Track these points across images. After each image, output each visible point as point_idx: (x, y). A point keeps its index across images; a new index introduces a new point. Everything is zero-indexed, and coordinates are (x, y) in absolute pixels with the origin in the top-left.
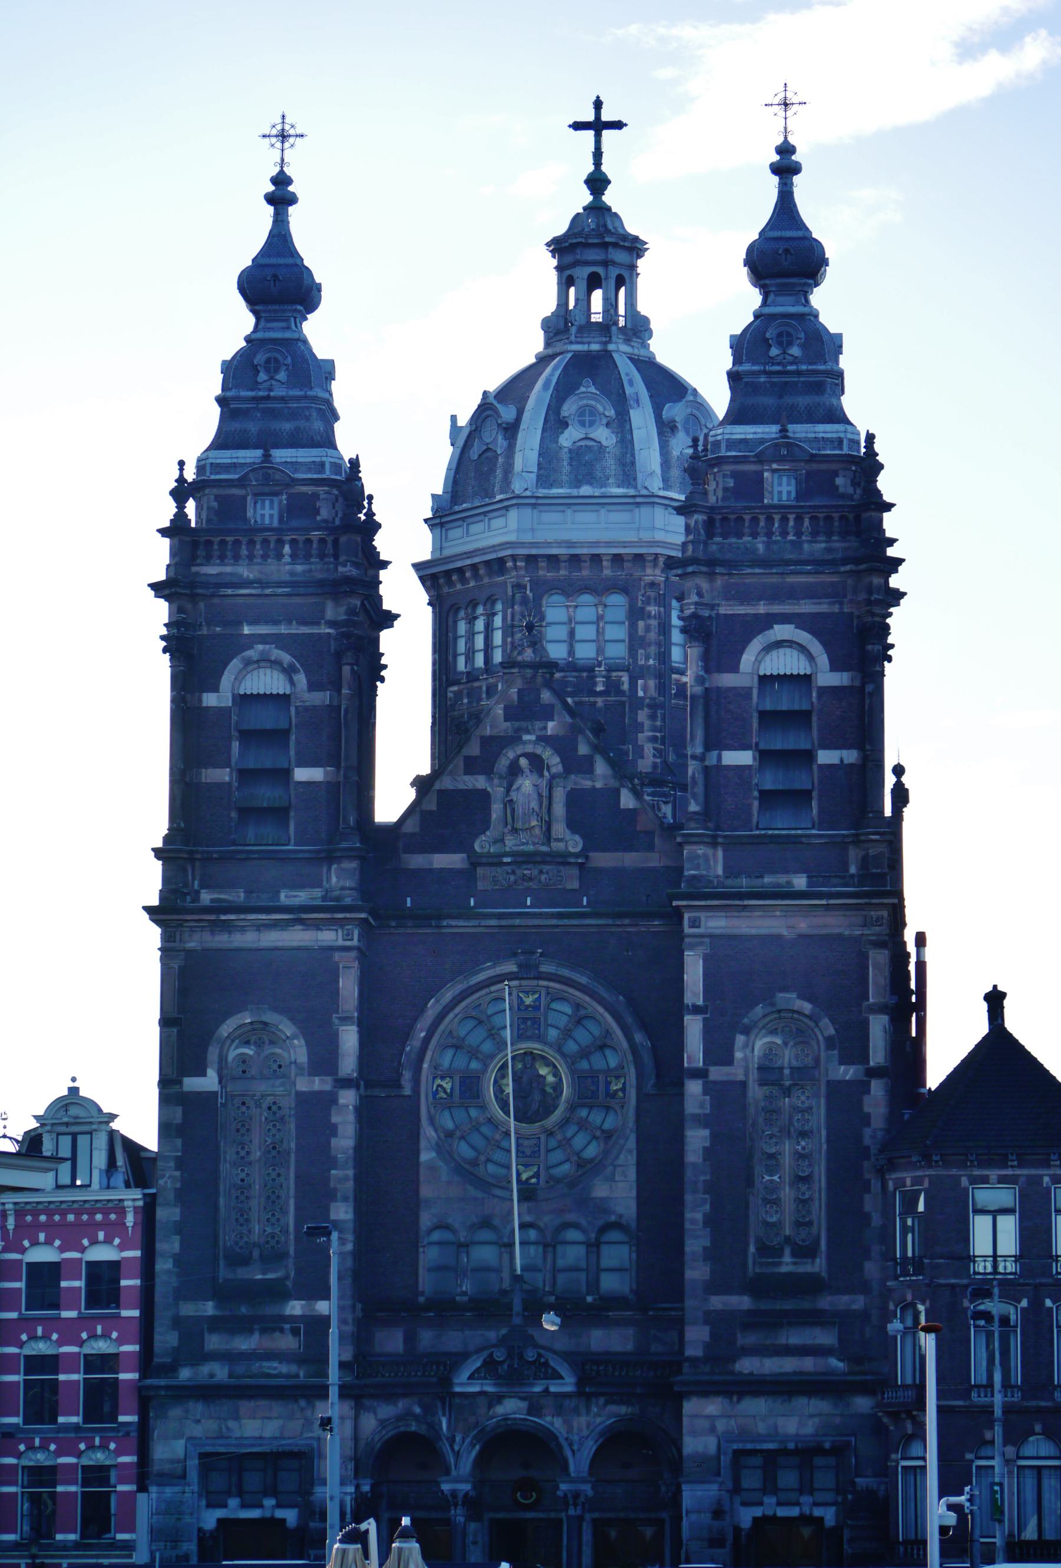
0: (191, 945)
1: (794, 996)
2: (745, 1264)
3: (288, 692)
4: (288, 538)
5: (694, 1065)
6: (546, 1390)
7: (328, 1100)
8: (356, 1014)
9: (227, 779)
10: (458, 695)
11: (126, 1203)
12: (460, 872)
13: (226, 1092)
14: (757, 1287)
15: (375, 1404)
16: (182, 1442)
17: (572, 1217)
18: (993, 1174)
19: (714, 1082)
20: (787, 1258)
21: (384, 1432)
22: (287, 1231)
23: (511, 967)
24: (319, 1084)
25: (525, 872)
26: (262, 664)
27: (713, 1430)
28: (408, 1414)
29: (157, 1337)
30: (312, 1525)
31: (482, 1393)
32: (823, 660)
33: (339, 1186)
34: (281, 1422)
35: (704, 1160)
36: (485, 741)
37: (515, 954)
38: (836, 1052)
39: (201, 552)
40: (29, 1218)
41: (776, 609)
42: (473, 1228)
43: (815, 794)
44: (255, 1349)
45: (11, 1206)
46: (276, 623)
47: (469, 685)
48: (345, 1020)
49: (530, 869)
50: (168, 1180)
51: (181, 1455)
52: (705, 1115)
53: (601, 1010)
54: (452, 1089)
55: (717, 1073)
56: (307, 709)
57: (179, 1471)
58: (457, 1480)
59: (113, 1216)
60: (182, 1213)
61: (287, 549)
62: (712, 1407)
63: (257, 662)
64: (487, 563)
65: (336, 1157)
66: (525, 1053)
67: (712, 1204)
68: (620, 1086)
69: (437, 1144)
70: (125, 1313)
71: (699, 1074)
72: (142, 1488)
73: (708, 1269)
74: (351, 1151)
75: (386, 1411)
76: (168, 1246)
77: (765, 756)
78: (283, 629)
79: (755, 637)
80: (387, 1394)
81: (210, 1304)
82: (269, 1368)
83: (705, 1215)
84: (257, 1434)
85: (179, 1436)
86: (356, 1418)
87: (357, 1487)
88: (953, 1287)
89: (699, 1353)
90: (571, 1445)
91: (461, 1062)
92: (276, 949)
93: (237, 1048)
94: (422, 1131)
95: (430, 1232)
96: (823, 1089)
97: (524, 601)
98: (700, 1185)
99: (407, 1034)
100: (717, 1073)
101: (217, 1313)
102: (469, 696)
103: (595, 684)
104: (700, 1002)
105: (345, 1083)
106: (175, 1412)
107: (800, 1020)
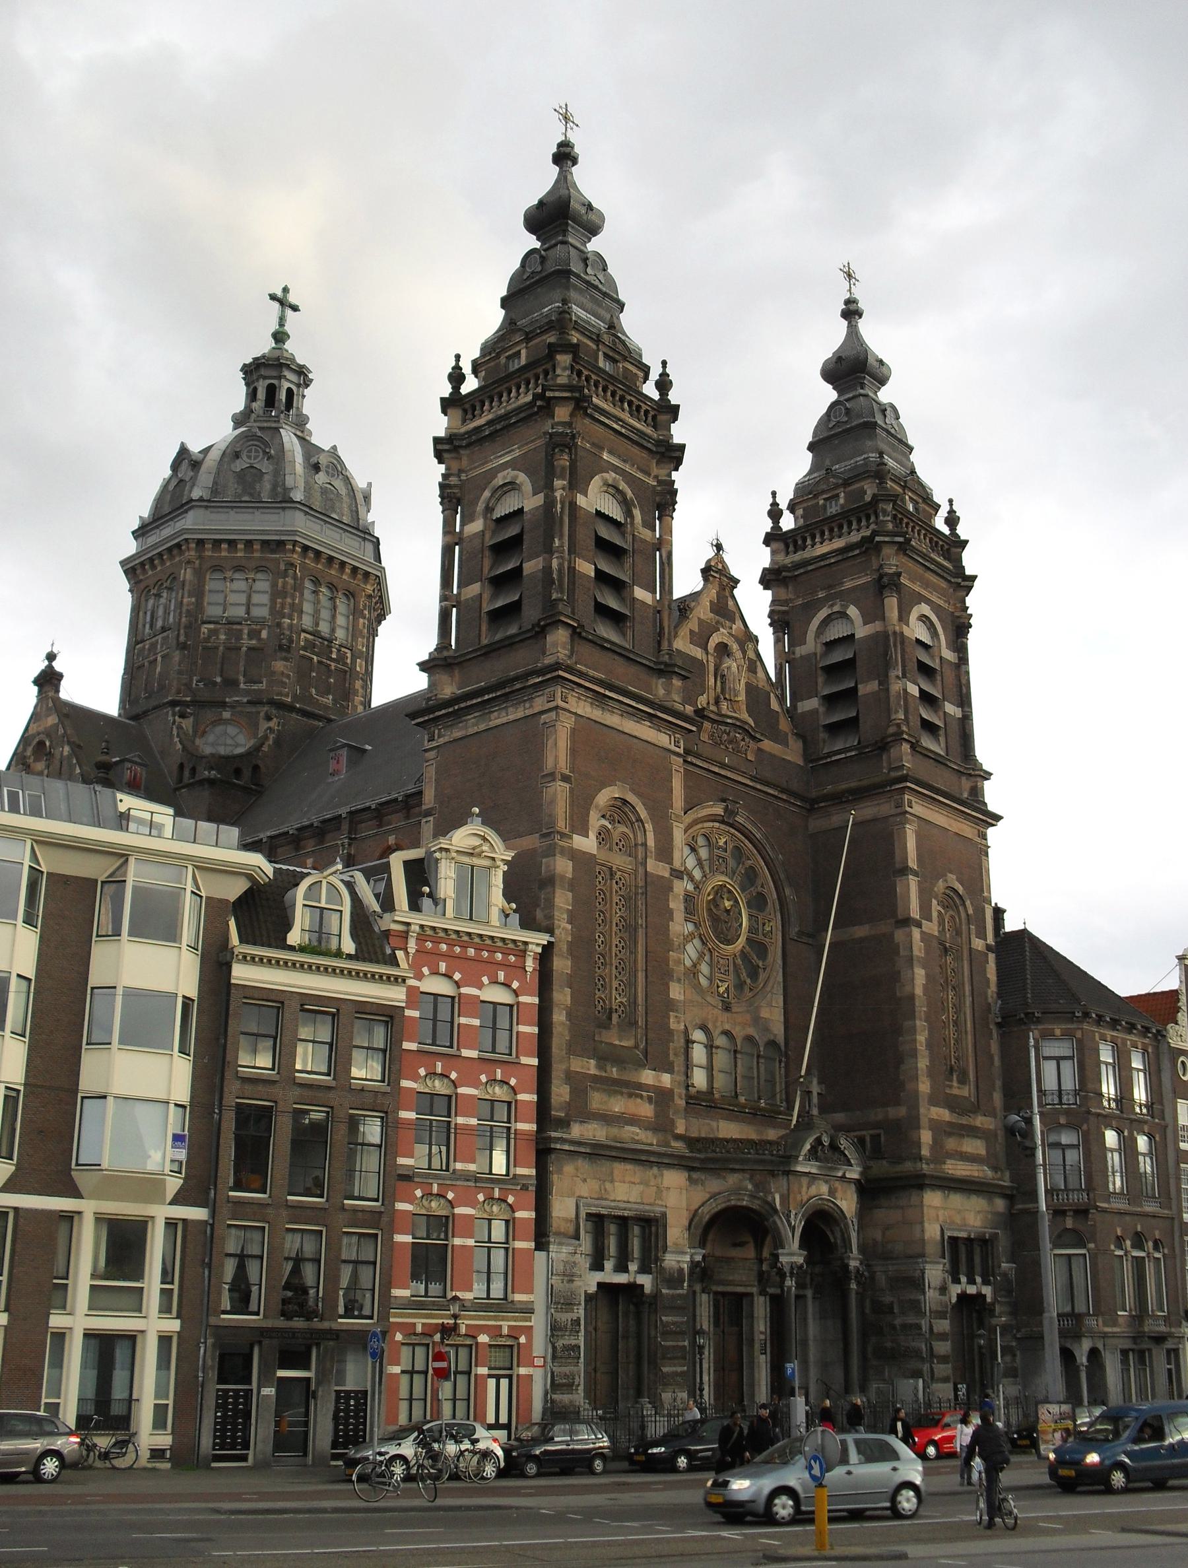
1: (955, 877)
6: (844, 1177)
14: (953, 1104)
17: (751, 1031)
18: (1110, 1033)
22: (635, 1002)
23: (719, 810)
26: (611, 490)
28: (737, 1191)
29: (554, 1089)
34: (641, 1187)
37: (724, 800)
40: (429, 945)
41: (924, 592)
43: (942, 732)
45: (417, 928)
46: (624, 461)
47: (227, 626)
57: (571, 1229)
58: (792, 1254)
63: (609, 485)
64: (265, 543)
70: (525, 1060)
71: (919, 925)
75: (715, 1185)
76: (562, 996)
78: (627, 468)
82: (633, 1133)
92: (635, 737)
97: (295, 577)
103: (331, 652)
106: (569, 1169)
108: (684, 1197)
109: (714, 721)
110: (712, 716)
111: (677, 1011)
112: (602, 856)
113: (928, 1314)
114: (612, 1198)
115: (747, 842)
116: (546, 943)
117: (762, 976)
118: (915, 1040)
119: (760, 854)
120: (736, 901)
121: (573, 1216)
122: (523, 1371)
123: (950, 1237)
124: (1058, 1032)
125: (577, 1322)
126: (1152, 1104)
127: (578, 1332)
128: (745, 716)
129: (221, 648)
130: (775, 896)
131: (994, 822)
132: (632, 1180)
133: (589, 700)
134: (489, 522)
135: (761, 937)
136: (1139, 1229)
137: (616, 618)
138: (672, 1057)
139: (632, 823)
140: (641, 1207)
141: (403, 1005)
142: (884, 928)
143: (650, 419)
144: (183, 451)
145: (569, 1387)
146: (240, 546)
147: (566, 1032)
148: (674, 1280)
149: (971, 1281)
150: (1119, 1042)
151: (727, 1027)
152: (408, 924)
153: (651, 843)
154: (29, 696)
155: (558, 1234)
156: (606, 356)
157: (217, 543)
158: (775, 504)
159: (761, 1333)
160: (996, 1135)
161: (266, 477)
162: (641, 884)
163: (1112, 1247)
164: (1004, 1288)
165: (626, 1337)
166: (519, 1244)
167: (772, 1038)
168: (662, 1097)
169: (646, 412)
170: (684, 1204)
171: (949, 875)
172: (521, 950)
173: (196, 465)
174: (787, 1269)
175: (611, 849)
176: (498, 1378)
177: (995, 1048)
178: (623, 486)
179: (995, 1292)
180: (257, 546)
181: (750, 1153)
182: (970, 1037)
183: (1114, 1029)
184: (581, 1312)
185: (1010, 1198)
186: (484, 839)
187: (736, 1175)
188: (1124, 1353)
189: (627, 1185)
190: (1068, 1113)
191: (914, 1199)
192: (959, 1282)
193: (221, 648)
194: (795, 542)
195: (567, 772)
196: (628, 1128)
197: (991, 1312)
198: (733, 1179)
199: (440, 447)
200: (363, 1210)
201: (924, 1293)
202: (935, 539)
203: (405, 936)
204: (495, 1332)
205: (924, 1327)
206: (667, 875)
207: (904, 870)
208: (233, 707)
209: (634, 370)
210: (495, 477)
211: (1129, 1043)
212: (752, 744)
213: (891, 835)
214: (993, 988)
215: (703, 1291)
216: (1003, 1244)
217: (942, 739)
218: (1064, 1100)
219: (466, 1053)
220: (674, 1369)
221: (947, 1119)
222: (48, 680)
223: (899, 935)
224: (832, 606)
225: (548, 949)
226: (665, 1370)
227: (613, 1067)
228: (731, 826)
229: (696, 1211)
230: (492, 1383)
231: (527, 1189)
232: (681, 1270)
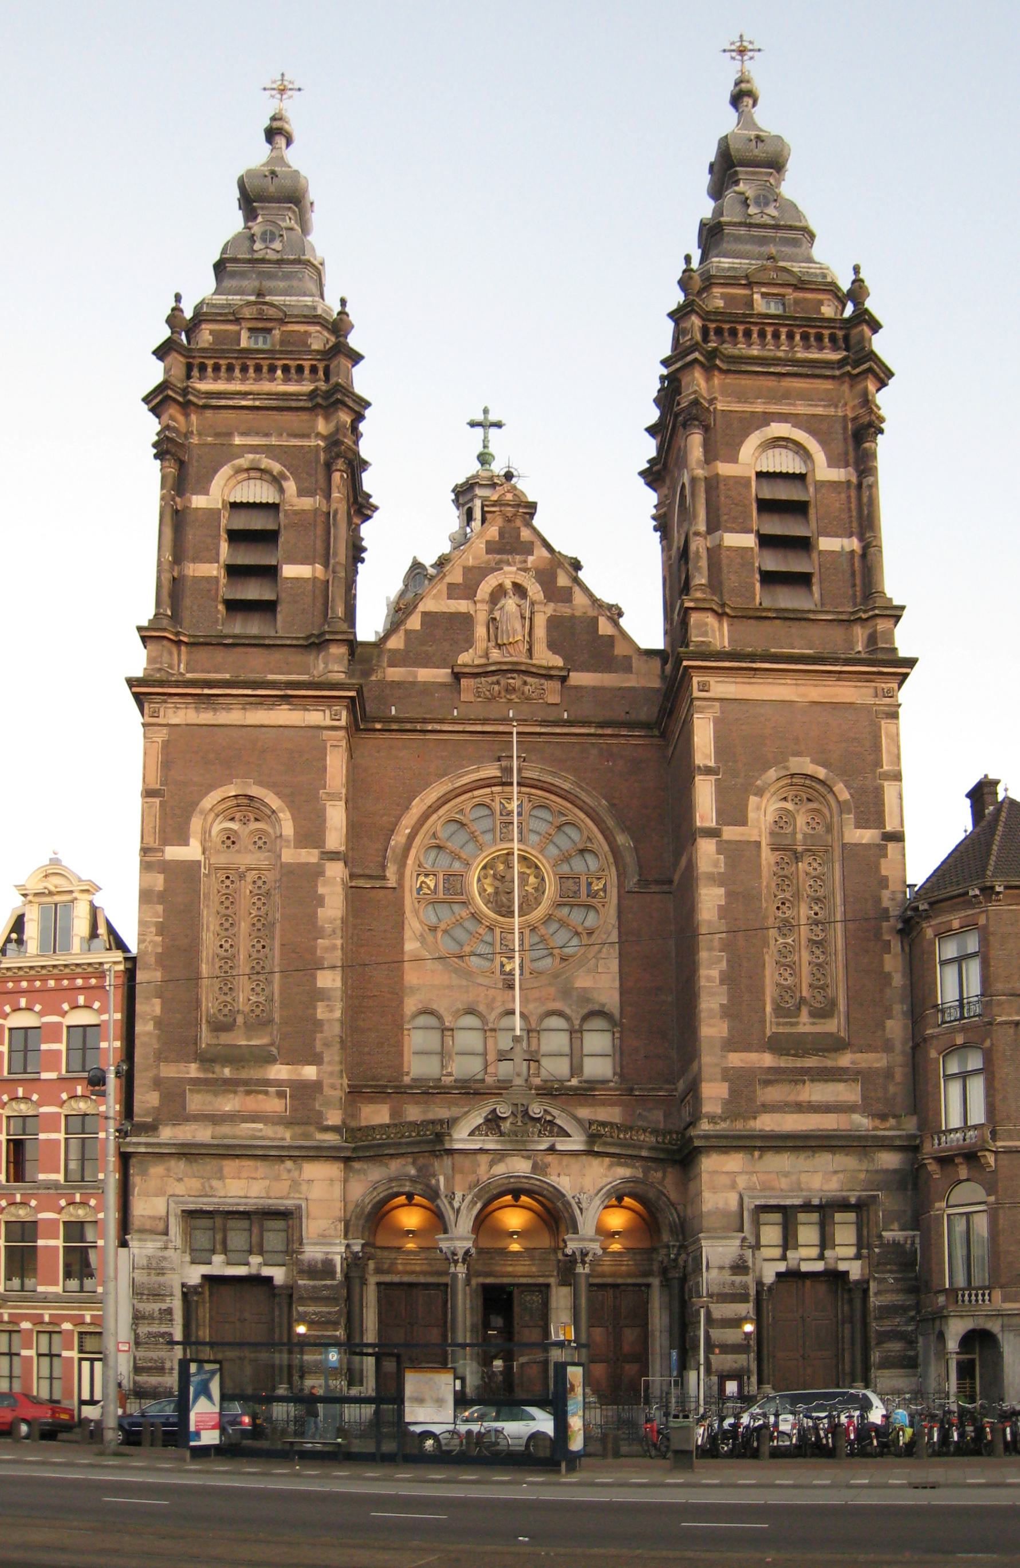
0: (174, 720)
2: (763, 1021)
7: (315, 873)
8: (344, 791)
9: (215, 573)
11: (106, 966)
13: (210, 864)
15: (365, 1167)
16: (165, 1199)
19: (727, 842)
20: (804, 1017)
22: (270, 1000)
24: (310, 856)
26: (253, 474)
29: (137, 1097)
30: (300, 1282)
33: (326, 956)
34: (267, 1182)
35: (720, 918)
37: (499, 759)
38: (852, 816)
39: (195, 373)
42: (458, 1014)
46: (267, 435)
48: (333, 797)
49: (513, 678)
51: (163, 1213)
52: (719, 873)
55: (730, 833)
56: (296, 513)
57: (161, 1226)
62: (734, 1162)
63: (248, 470)
65: (323, 927)
67: (728, 961)
68: (601, 886)
71: (712, 833)
73: (726, 1026)
74: (339, 922)
76: (148, 1008)
77: (766, 541)
78: (274, 441)
79: (752, 432)
81: (193, 1066)
82: (253, 1129)
83: (721, 972)
84: (242, 1194)
86: (346, 1181)
87: (348, 1246)
89: (719, 1110)
90: (579, 1203)
94: (406, 922)
96: (837, 852)
98: (716, 944)
99: (391, 831)
100: (730, 833)
101: (201, 1075)
105: (333, 856)
106: (157, 1170)
108: (337, 1190)
111: (329, 999)
112: (221, 859)
114: (222, 1194)
119: (576, 806)
130: (606, 848)
132: (253, 1175)
133: (193, 706)
137: (268, 608)
138: (318, 1049)
139: (269, 817)
140: (261, 1201)
145: (160, 1369)
153: (288, 828)
155: (141, 1231)
172: (99, 971)
177: (893, 963)
178: (266, 463)
184: (177, 1304)
187: (398, 1161)
189: (244, 1181)
195: (158, 787)
198: (395, 1166)
227: (223, 1066)
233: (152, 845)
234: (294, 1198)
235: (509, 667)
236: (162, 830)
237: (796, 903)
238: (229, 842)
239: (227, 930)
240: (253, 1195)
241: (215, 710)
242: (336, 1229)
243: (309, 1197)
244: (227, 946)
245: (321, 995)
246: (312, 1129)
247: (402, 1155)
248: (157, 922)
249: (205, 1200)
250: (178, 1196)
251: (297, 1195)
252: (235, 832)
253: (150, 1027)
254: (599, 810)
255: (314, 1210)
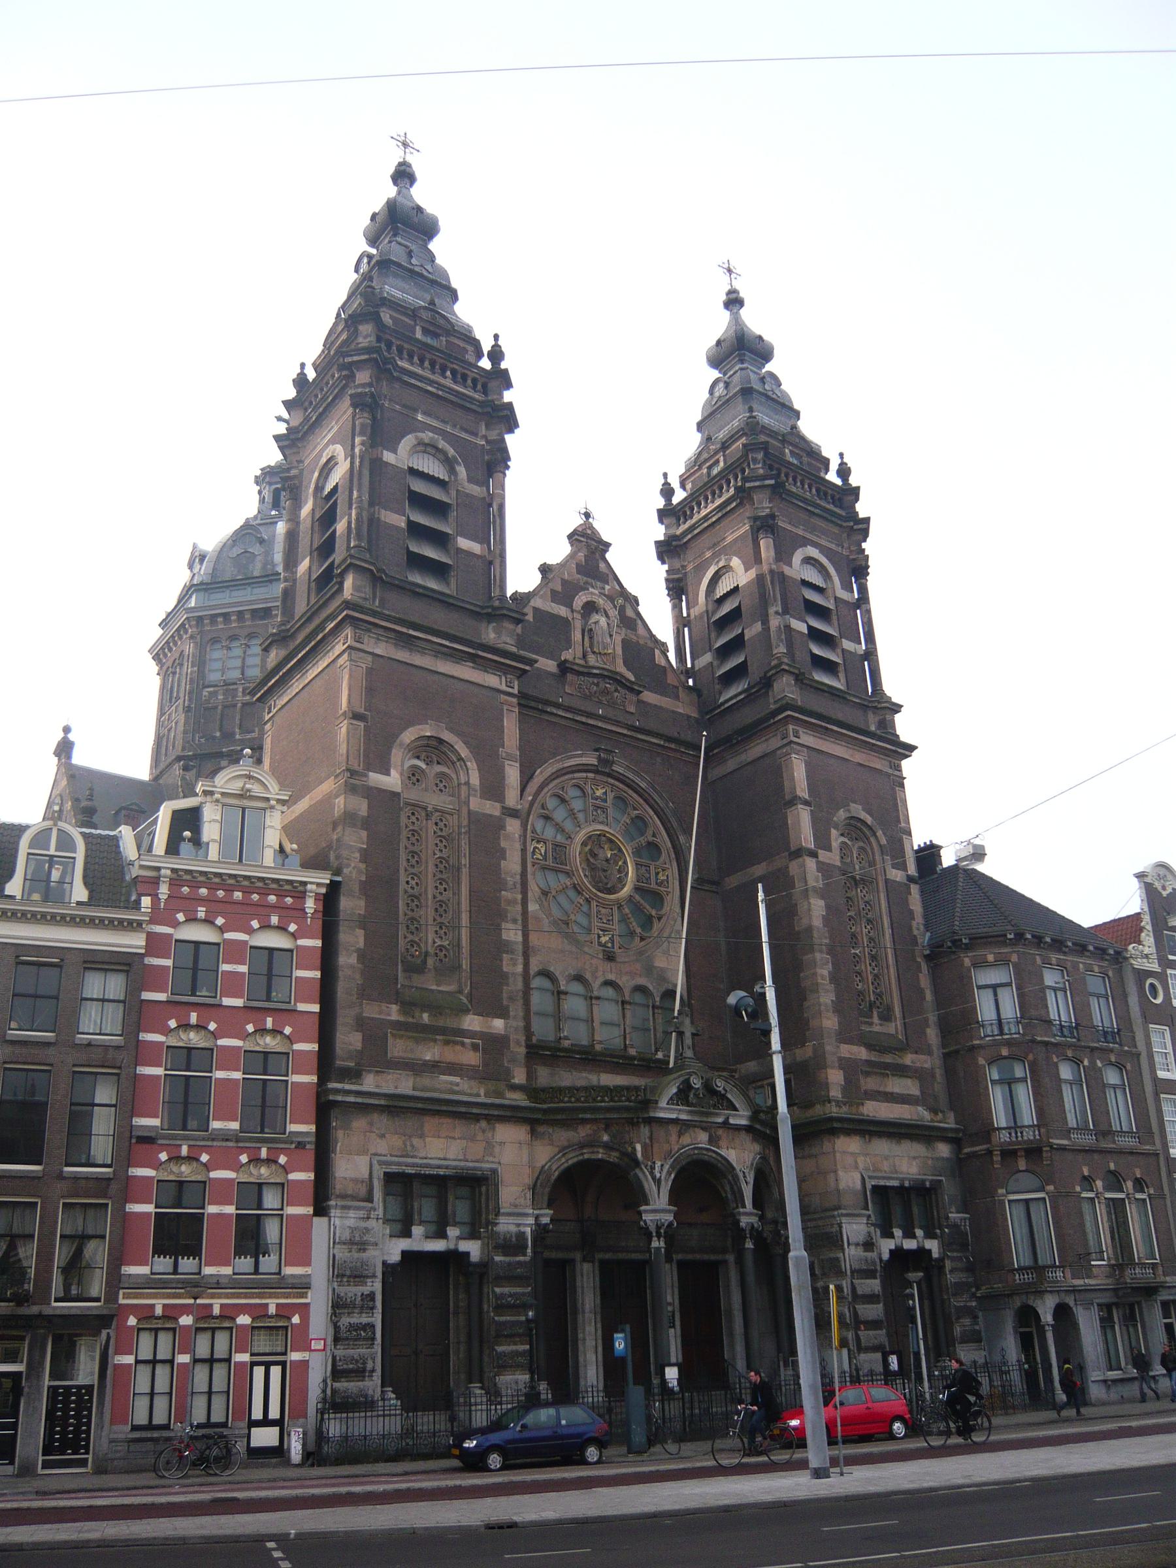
0: (378, 651)
3: (447, 479)
4: (452, 366)
5: (809, 846)
6: (726, 1123)
10: (215, 693)
11: (309, 887)
12: (553, 674)
15: (550, 1130)
16: (367, 1158)
18: (1054, 957)
21: (563, 1160)
22: (459, 945)
24: (491, 808)
25: (608, 686)
26: (429, 449)
27: (857, 1168)
28: (591, 1143)
30: (497, 1258)
31: (675, 1121)
32: (836, 580)
35: (824, 926)
36: (564, 583)
37: (596, 750)
40: (186, 890)
41: (808, 536)
43: (841, 668)
44: (438, 1062)
45: (168, 872)
46: (443, 421)
48: (510, 757)
50: (354, 871)
53: (652, 813)
54: (545, 853)
56: (467, 495)
57: (363, 1191)
59: (289, 900)
60: (366, 907)
61: (448, 373)
64: (254, 612)
66: (599, 835)
69: (539, 898)
70: (302, 1007)
71: (814, 854)
72: (321, 1210)
75: (563, 1136)
76: (352, 939)
80: (567, 1119)
81: (394, 1008)
82: (451, 1083)
85: (363, 1151)
87: (537, 1218)
88: (1046, 1044)
91: (549, 833)
93: (409, 759)
95: (534, 976)
96: (881, 885)
100: (823, 855)
101: (401, 1019)
102: (224, 694)
104: (807, 797)
106: (359, 1123)
107: (860, 830)
109: (579, 673)
110: (575, 667)
111: (512, 952)
112: (413, 795)
113: (849, 1272)
114: (421, 1155)
115: (630, 792)
116: (328, 882)
117: (657, 926)
118: (815, 974)
120: (620, 850)
121: (367, 1176)
122: (295, 1356)
123: (875, 1188)
124: (991, 958)
125: (371, 1296)
126: (1119, 1030)
127: (372, 1308)
128: (621, 668)
129: (220, 707)
131: (907, 753)
132: (451, 1135)
134: (319, 500)
135: (653, 886)
136: (1112, 1166)
137: (439, 570)
138: (505, 1003)
140: (462, 1164)
141: (143, 951)
142: (779, 863)
143: (479, 387)
144: (195, 546)
145: (360, 1373)
146: (233, 618)
147: (358, 976)
148: (514, 1245)
149: (909, 1234)
150: (1069, 965)
151: (611, 977)
152: (158, 869)
153: (475, 780)
154: (50, 765)
155: (343, 1196)
156: (425, 331)
157: (213, 618)
158: (666, 484)
159: (670, 1304)
160: (933, 1076)
161: (259, 558)
162: (465, 823)
163: (1078, 1189)
164: (955, 1241)
165: (456, 1313)
166: (291, 1210)
167: (670, 987)
168: (493, 1045)
169: (474, 381)
170: (525, 1159)
171: (852, 805)
172: (298, 891)
173: (202, 557)
174: (653, 1228)
175: (426, 790)
176: (267, 1366)
177: (925, 981)
178: (442, 444)
179: (944, 1246)
180: (247, 616)
181: (602, 1101)
182: (892, 970)
183: (1060, 951)
184: (377, 1286)
185: (956, 1142)
186: (250, 777)
187: (588, 1126)
188: (1108, 1307)
190: (1009, 1043)
191: (827, 1146)
192: (892, 1236)
193: (220, 707)
194: (685, 513)
195: (362, 711)
196: (443, 1078)
197: (941, 1268)
198: (584, 1132)
199: (281, 444)
200: (87, 1178)
201: (843, 1250)
202: (823, 488)
203: (155, 882)
204: (259, 1313)
205: (845, 1290)
206: (497, 813)
207: (794, 801)
208: (228, 756)
209: (462, 344)
210: (322, 456)
211: (1081, 965)
212: (630, 696)
213: (779, 768)
214: (919, 919)
215: (584, 1260)
216: (950, 1189)
217: (842, 675)
218: (1006, 1030)
219: (227, 1001)
220: (514, 1348)
221: (864, 1058)
222: (64, 749)
223: (794, 868)
224: (718, 562)
225: (334, 887)
226: (500, 1349)
227: (423, 1011)
228: (609, 775)
229: (543, 1167)
230: (259, 1372)
231: (304, 1147)
232: (521, 1236)
233: (356, 768)
234: (488, 1161)
235: (610, 674)
236: (366, 756)
237: (858, 921)
238: (414, 779)
239: (413, 866)
240: (451, 1157)
241: (411, 650)
242: (525, 1199)
243: (502, 1162)
244: (413, 883)
245: (504, 947)
246: (502, 1086)
247: (595, 1121)
248: (361, 848)
249: (410, 1160)
250: (380, 1155)
251: (491, 1159)
252: (423, 771)
253: (353, 960)
254: (668, 811)
255: (505, 1175)
